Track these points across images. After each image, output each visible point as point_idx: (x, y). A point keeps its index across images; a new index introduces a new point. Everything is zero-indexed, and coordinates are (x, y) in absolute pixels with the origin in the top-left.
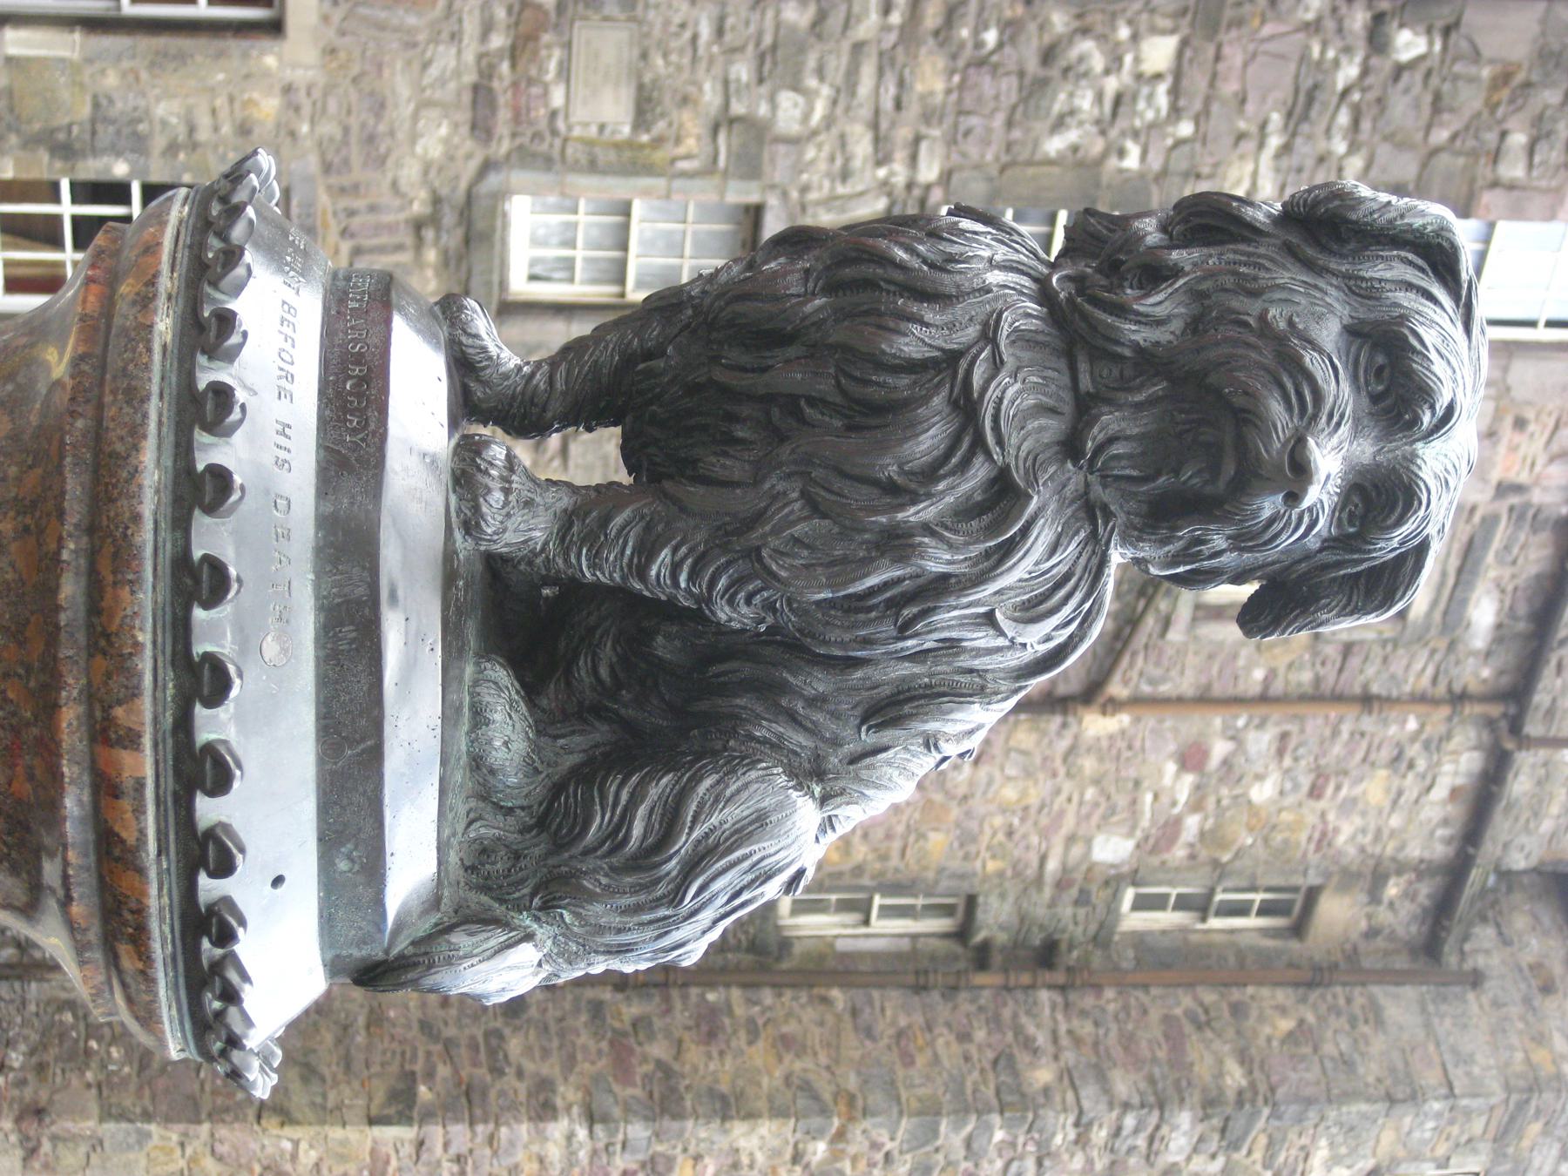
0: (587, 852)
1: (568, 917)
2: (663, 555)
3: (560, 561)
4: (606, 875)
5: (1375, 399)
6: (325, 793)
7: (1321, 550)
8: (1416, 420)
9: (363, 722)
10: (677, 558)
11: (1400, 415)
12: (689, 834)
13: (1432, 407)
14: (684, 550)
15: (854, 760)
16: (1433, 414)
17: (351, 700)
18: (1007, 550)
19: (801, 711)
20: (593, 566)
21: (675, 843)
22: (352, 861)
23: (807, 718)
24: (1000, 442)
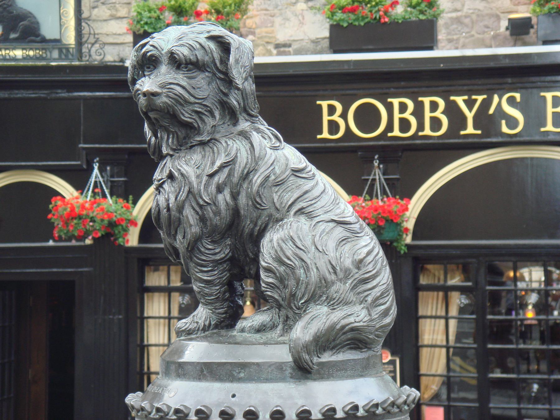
0: (280, 296)
1: (303, 301)
2: (199, 276)
3: (214, 305)
4: (286, 290)
5: (155, 68)
6: (216, 380)
7: (207, 71)
8: (152, 56)
9: (198, 368)
10: (199, 271)
11: (154, 60)
12: (270, 264)
13: (148, 52)
14: (196, 270)
15: (277, 209)
16: (150, 51)
17: (193, 371)
18: (182, 175)
19: (258, 228)
20: (212, 295)
21: (273, 269)
22: (240, 372)
23: (261, 226)
24: (162, 179)
